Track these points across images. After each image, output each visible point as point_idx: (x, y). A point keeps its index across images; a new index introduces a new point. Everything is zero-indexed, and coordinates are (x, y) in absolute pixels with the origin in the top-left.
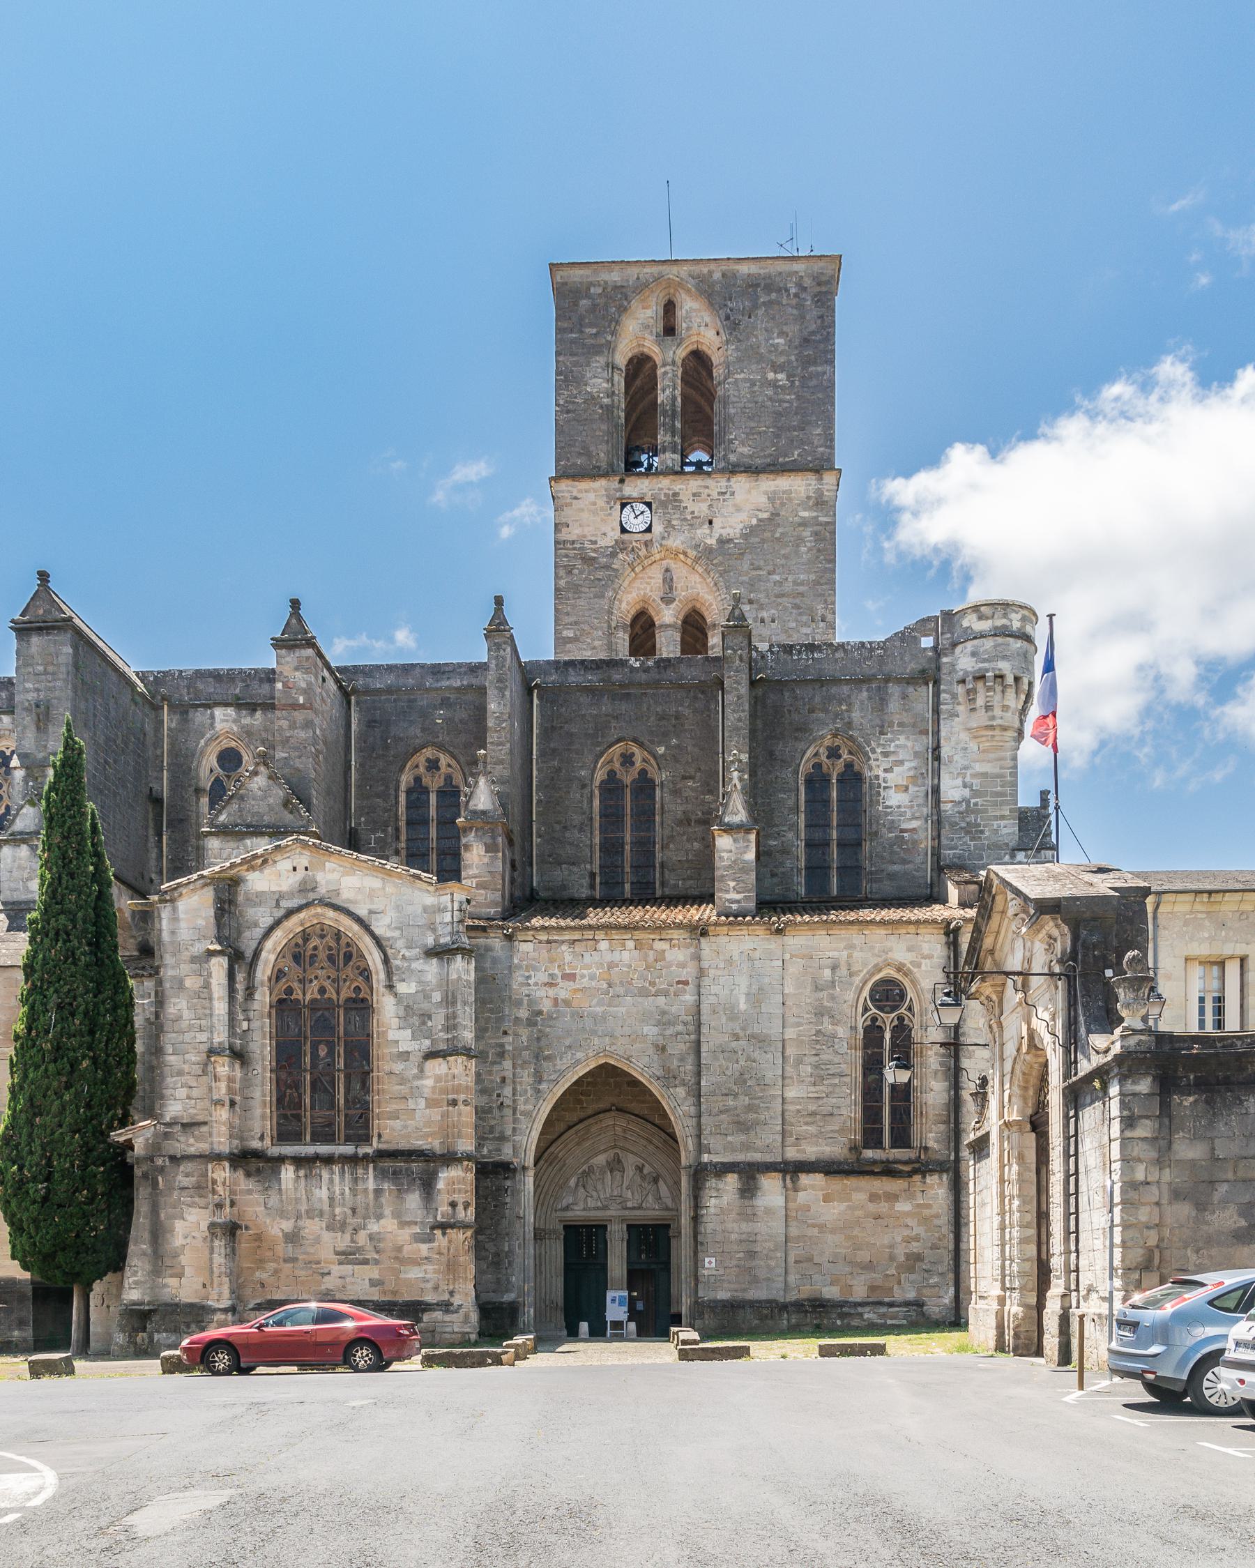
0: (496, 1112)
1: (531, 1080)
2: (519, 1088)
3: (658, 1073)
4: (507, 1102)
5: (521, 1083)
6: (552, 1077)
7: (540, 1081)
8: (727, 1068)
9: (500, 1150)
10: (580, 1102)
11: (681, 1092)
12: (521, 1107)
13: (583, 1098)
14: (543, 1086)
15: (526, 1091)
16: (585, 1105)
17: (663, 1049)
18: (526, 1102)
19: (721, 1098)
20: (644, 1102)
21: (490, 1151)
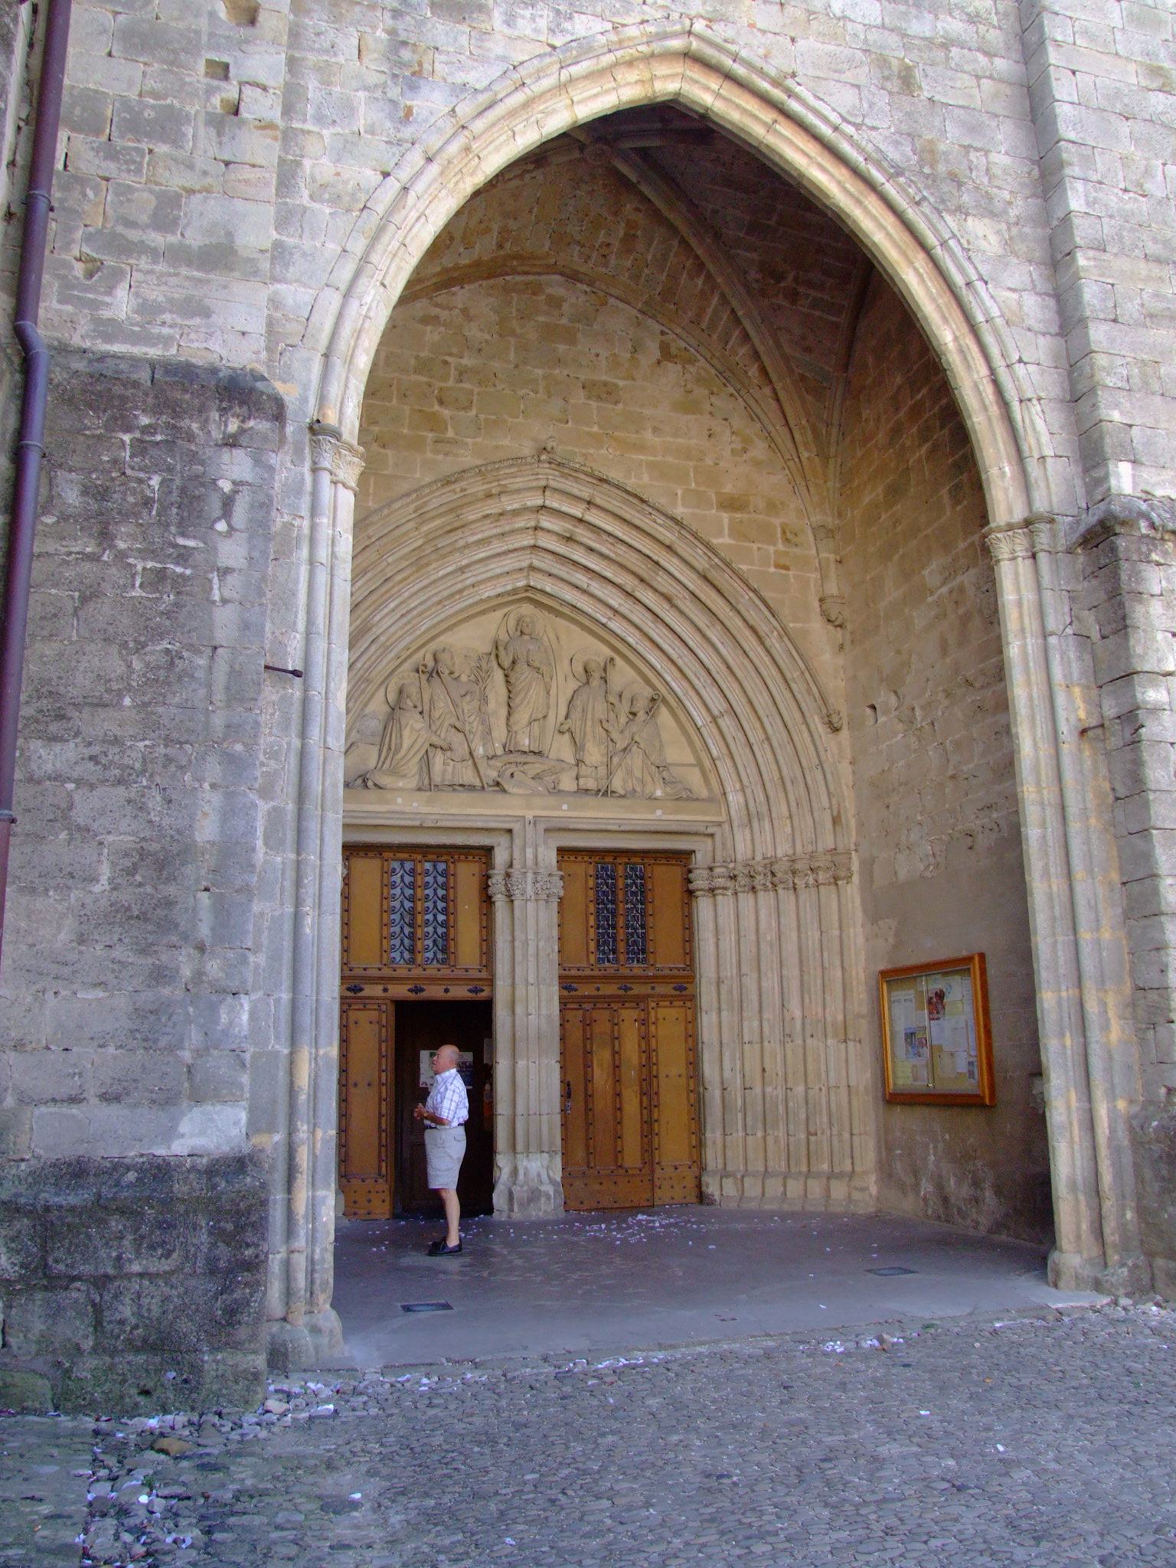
0: (201, 141)
1: (373, 69)
2: (312, 85)
3: (893, 154)
4: (261, 106)
5: (325, 73)
6: (476, 77)
7: (414, 78)
8: (1148, 172)
9: (206, 313)
10: (435, 423)
11: (984, 235)
12: (318, 165)
13: (446, 413)
14: (431, 102)
15: (348, 109)
16: (450, 434)
17: (907, 81)
18: (347, 147)
19: (1143, 268)
20: (640, 448)
21: (148, 310)
